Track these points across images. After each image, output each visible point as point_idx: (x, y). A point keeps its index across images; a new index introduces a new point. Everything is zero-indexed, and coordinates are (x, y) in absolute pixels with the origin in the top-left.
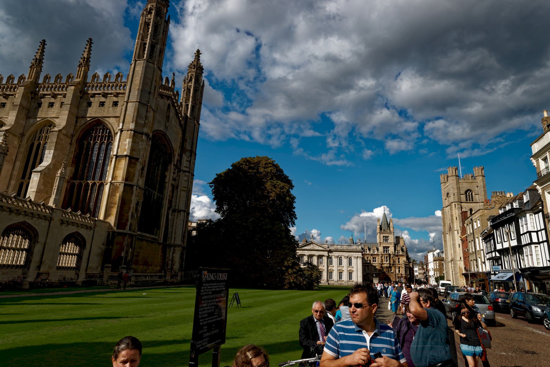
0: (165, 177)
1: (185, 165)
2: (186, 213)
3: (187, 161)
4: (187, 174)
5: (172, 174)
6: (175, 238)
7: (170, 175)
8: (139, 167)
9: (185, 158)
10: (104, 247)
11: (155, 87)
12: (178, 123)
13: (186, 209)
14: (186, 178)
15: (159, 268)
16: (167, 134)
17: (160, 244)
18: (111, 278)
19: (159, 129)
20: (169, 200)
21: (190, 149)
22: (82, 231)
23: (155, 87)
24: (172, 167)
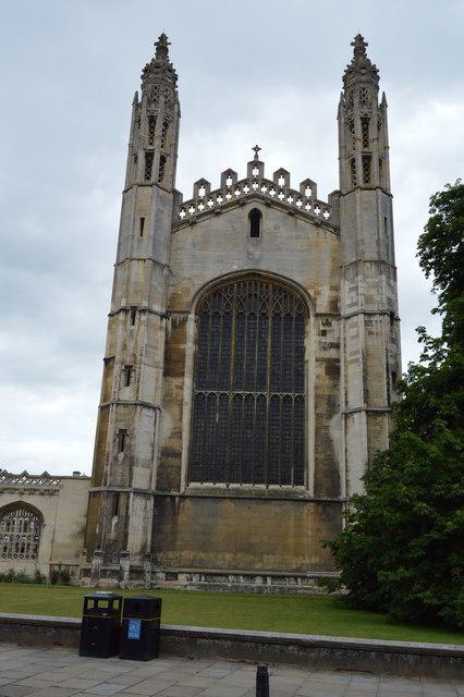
0: (301, 351)
1: (348, 302)
2: (363, 413)
3: (351, 289)
4: (355, 319)
5: (318, 338)
6: (347, 481)
7: (312, 344)
8: (117, 368)
9: (346, 286)
10: (83, 521)
11: (142, 220)
12: (308, 226)
13: (363, 405)
14: (352, 332)
15: (315, 560)
16: (263, 266)
17: (305, 501)
18: (86, 572)
19: (224, 272)
20: (318, 397)
21: (354, 260)
22: (33, 500)
23: (142, 220)
24: (312, 327)
